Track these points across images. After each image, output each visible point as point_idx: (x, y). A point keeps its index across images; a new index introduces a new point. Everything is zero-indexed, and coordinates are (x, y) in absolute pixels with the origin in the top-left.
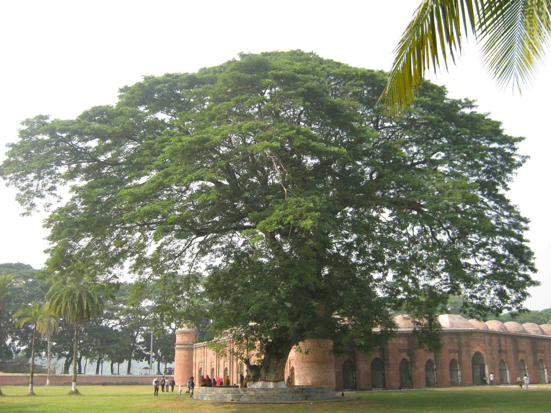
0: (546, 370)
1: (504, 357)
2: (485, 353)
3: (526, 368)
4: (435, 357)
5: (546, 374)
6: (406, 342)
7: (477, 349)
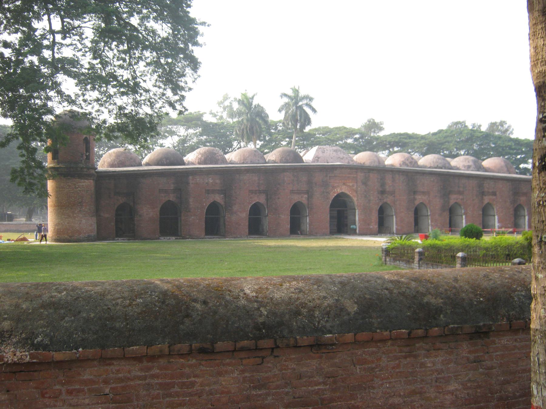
0: (464, 217)
1: (388, 199)
2: (355, 194)
3: (429, 214)
4: (267, 200)
5: (464, 221)
6: (218, 181)
7: (344, 189)
